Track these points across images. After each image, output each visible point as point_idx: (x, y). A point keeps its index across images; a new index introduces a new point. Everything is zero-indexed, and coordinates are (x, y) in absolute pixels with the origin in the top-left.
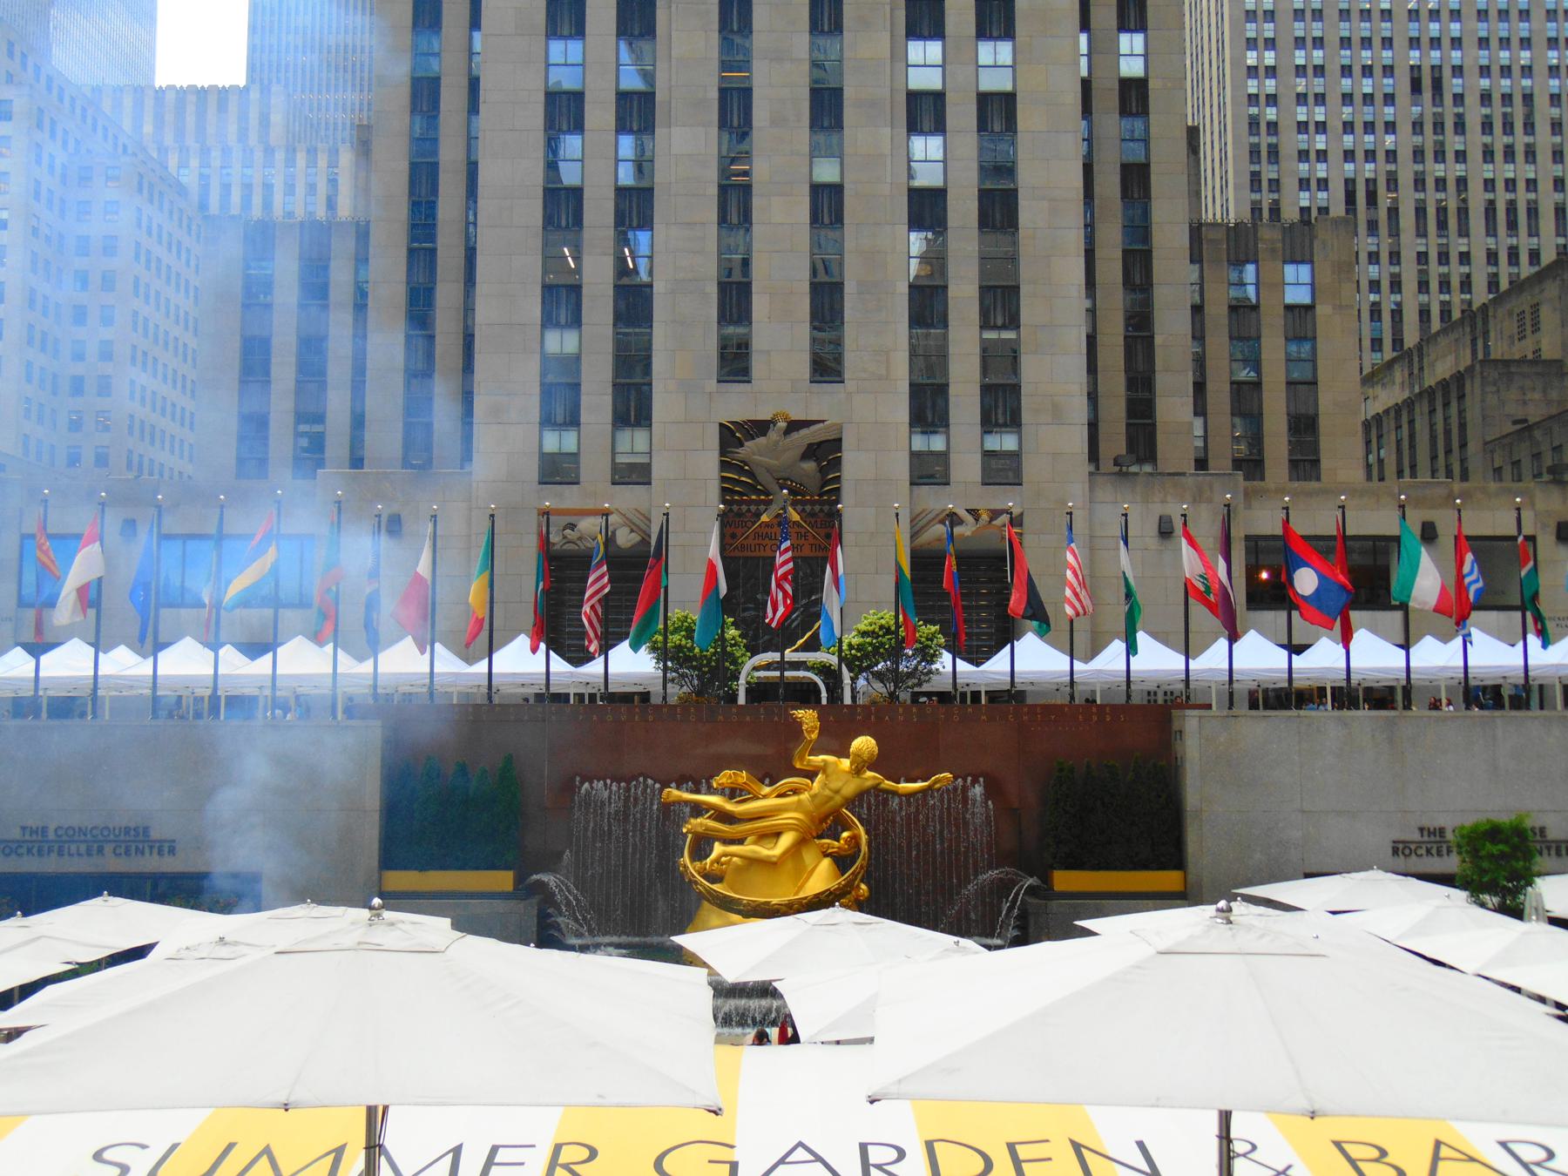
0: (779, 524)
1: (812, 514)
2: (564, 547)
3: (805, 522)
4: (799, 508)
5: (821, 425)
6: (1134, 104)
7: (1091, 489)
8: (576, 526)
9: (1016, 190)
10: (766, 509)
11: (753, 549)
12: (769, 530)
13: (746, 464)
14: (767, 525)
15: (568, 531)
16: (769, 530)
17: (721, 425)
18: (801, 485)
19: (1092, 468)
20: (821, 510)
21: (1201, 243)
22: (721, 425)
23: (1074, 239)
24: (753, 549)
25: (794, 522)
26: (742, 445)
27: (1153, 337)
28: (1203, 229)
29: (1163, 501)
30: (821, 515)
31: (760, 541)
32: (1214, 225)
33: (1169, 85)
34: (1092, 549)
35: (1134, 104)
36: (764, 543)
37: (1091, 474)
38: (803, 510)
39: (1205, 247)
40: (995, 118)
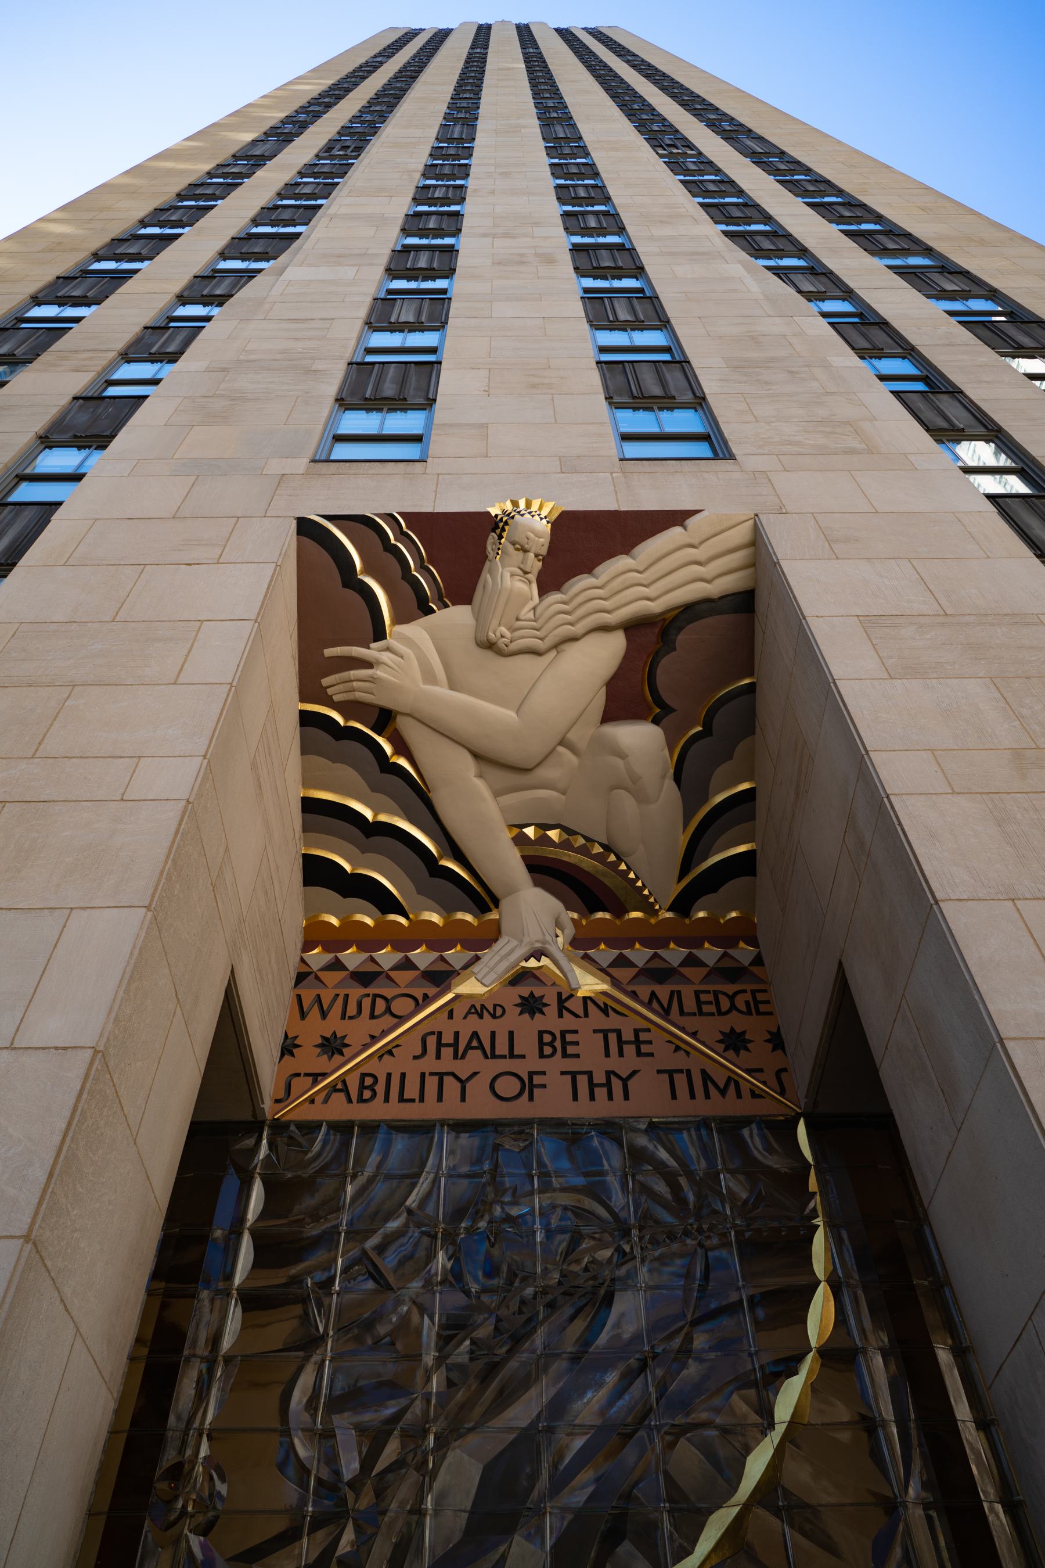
0: (531, 1006)
1: (658, 973)
3: (634, 995)
4: (605, 954)
5: (677, 530)
10: (477, 958)
11: (412, 1090)
12: (484, 1026)
13: (402, 748)
14: (477, 1009)
16: (484, 1026)
17: (305, 527)
18: (608, 848)
20: (691, 961)
22: (305, 527)
24: (412, 1090)
25: (585, 999)
26: (379, 634)
30: (694, 973)
31: (447, 1062)
36: (463, 1069)
38: (622, 961)
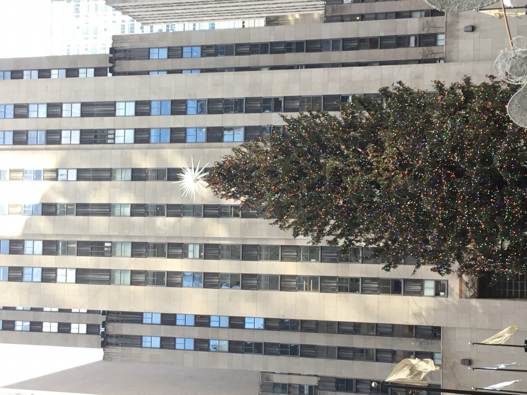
2: (476, 288)
6: (281, 48)
7: (452, 61)
8: (467, 283)
9: (324, 96)
15: (469, 285)
19: (442, 61)
21: (334, 16)
23: (305, 73)
27: (381, 37)
28: (327, 15)
29: (458, 30)
32: (326, 11)
33: (273, 33)
34: (479, 60)
35: (281, 48)
37: (445, 62)
39: (335, 14)
40: (294, 105)
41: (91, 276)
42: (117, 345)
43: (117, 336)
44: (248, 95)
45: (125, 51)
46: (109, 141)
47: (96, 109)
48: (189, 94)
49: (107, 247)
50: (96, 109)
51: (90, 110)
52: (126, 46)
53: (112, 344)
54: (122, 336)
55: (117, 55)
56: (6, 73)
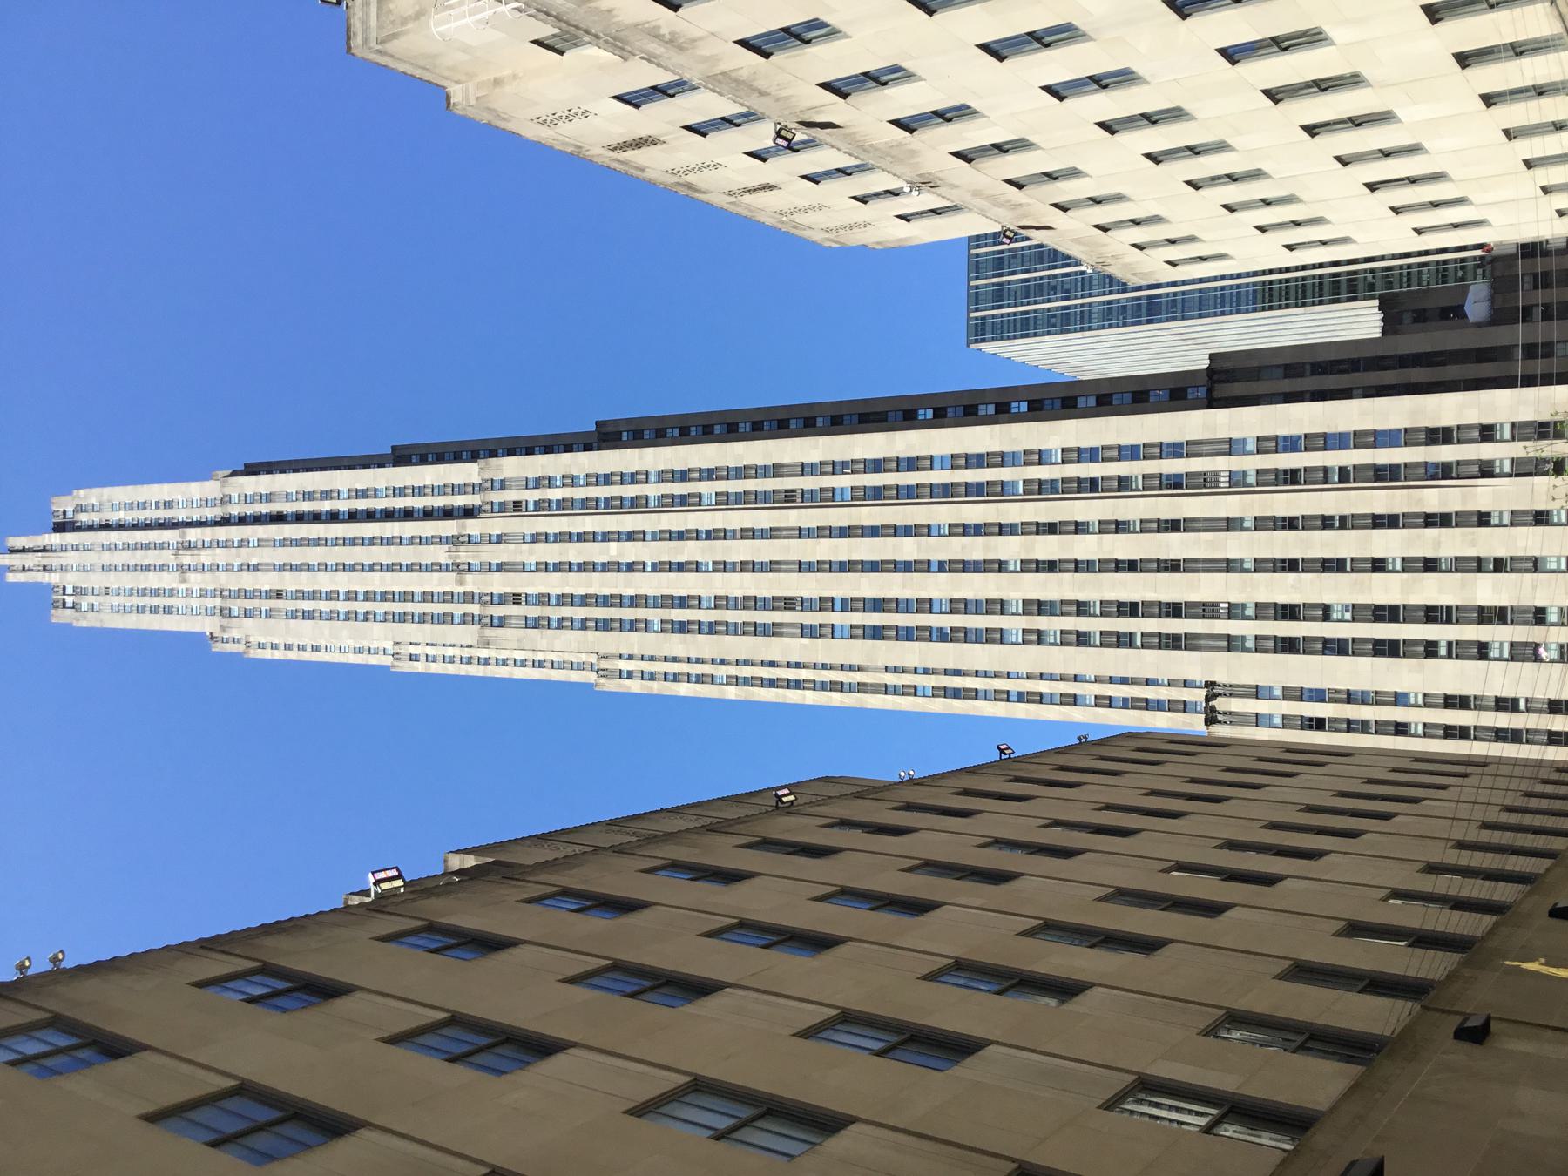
41: (1203, 642)
42: (1225, 723)
43: (1225, 713)
44: (1408, 425)
45: (1227, 372)
46: (1222, 485)
47: (1205, 448)
48: (1329, 426)
49: (1222, 608)
50: (1205, 448)
51: (1196, 449)
52: (1228, 365)
53: (1220, 722)
54: (1231, 713)
55: (1216, 377)
56: (1055, 400)
